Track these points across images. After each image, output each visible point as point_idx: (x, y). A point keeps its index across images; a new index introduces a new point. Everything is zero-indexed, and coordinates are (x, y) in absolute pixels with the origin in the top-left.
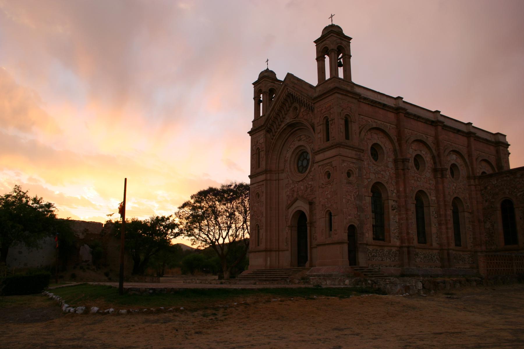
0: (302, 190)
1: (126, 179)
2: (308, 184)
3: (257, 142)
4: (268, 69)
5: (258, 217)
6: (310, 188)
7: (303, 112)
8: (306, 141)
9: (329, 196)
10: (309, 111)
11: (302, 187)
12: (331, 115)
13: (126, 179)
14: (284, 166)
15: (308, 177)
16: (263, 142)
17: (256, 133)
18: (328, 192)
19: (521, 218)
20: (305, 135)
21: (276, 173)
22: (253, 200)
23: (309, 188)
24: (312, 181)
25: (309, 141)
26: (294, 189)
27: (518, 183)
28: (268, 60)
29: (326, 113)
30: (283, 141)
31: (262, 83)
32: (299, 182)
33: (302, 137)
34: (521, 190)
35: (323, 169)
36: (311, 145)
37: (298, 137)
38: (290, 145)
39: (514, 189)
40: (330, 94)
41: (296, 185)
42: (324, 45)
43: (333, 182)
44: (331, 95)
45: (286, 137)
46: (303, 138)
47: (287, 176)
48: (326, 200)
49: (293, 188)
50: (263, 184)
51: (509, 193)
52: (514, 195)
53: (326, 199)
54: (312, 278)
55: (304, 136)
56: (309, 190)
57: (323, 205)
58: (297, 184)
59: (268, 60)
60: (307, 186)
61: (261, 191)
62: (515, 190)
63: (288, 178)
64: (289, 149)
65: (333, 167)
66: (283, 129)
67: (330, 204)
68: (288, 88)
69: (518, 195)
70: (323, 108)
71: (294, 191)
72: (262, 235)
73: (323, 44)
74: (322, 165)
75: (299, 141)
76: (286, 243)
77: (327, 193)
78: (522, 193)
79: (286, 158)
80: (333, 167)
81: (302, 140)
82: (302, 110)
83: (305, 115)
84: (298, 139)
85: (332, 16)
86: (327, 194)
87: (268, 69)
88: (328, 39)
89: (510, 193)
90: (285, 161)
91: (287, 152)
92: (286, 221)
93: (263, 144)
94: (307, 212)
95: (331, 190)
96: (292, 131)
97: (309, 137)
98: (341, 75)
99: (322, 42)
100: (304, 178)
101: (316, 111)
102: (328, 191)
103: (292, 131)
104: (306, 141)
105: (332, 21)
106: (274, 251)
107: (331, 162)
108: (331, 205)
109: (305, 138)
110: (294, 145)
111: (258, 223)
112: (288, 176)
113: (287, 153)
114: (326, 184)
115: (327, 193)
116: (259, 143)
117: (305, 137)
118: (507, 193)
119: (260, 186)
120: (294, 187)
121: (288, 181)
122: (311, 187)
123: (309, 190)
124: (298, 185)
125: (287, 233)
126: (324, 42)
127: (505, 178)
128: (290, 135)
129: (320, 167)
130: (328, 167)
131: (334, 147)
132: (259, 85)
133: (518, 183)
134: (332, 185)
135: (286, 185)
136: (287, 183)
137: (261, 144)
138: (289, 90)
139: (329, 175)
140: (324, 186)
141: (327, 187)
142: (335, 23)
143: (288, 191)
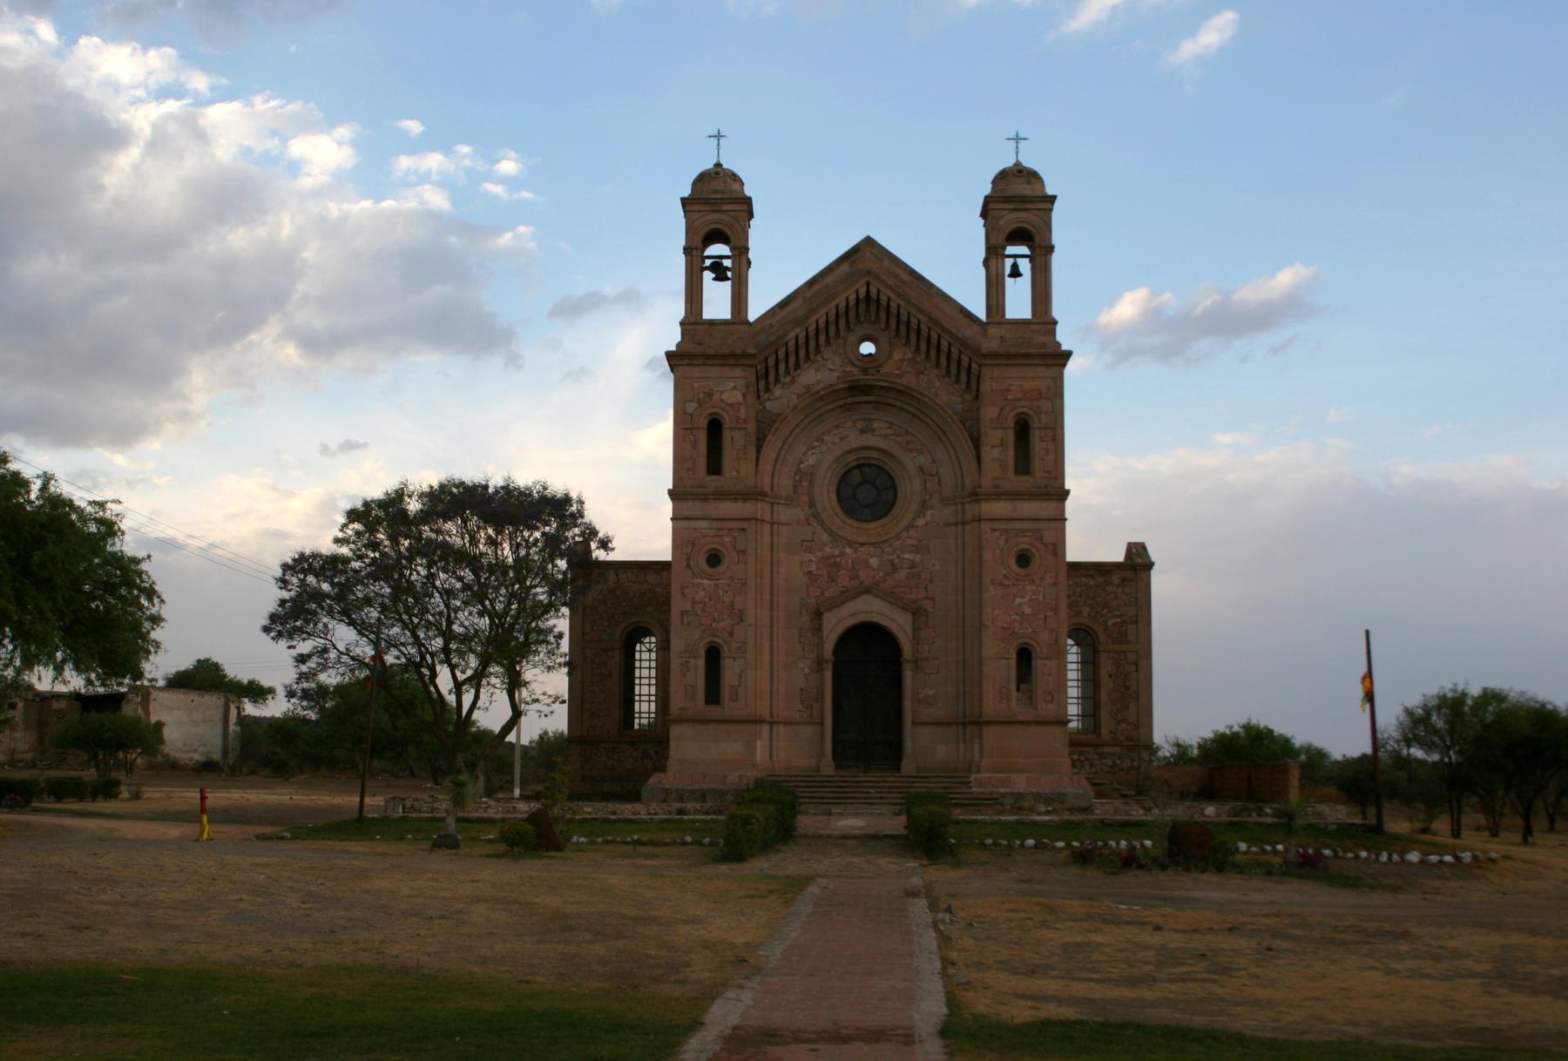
0: (873, 569)
1: (1367, 632)
2: (899, 557)
3: (710, 395)
4: (718, 165)
5: (714, 620)
6: (906, 571)
7: (903, 361)
8: (896, 442)
9: (1027, 610)
10: (925, 368)
11: (874, 562)
12: (1043, 416)
13: (1367, 632)
14: (795, 486)
15: (899, 539)
16: (740, 404)
17: (704, 365)
18: (1025, 600)
19: (1110, 676)
20: (890, 423)
21: (772, 504)
22: (688, 566)
23: (902, 568)
24: (916, 553)
25: (908, 443)
26: (838, 560)
27: (1113, 595)
28: (719, 136)
29: (1024, 403)
30: (806, 418)
31: (731, 214)
32: (862, 544)
33: (875, 424)
34: (1117, 613)
35: (1007, 541)
36: (914, 457)
37: (863, 420)
38: (824, 434)
39: (1103, 610)
40: (1042, 363)
41: (848, 550)
42: (1021, 222)
43: (1041, 579)
44: (1046, 365)
45: (822, 410)
46: (880, 428)
47: (807, 520)
48: (1017, 618)
49: (831, 556)
50: (744, 530)
51: (1089, 615)
52: (1101, 621)
53: (1017, 614)
54: (1101, 803)
55: (887, 425)
56: (903, 573)
57: (1003, 628)
58: (850, 547)
59: (719, 136)
60: (896, 561)
61: (734, 547)
62: (1105, 611)
63: (809, 524)
64: (816, 444)
65: (1045, 545)
66: (830, 390)
67: (1030, 630)
68: (872, 280)
69: (1110, 623)
70: (1012, 388)
71: (836, 565)
72: (740, 676)
73: (1015, 215)
74: (1006, 531)
75: (862, 431)
76: (802, 702)
77: (1018, 601)
78: (1119, 620)
79: (802, 466)
80: (1045, 545)
81: (877, 432)
82: (897, 356)
83: (909, 372)
84: (860, 427)
85: (1017, 139)
86: (1020, 604)
87: (718, 165)
88: (1036, 212)
89: (1093, 615)
90: (796, 474)
91: (809, 449)
92: (800, 642)
93: (743, 409)
94: (904, 631)
95: (1034, 597)
96: (849, 400)
97: (907, 433)
98: (1018, 303)
99: (1016, 210)
100: (885, 537)
101: (987, 386)
102: (1023, 597)
103: (849, 400)
104: (896, 442)
105: (1017, 153)
106: (767, 722)
107: (1038, 530)
108: (1034, 632)
109: (890, 432)
110: (842, 439)
111: (717, 640)
112: (811, 518)
113: (810, 453)
114: (1018, 580)
115: (1018, 601)
116: (722, 400)
117: (890, 428)
118: (1086, 615)
119: (725, 532)
120: (837, 553)
121: (813, 533)
122: (912, 567)
123: (903, 573)
124: (856, 554)
125: (805, 675)
126: (1022, 215)
127: (1083, 579)
128: (833, 409)
129: (997, 534)
130: (1027, 539)
131: (1052, 497)
132: (717, 216)
133: (1113, 595)
134: (1037, 586)
135: (803, 541)
136: (811, 539)
137: (731, 405)
138: (873, 291)
139: (1024, 560)
140: (1010, 583)
141: (1020, 587)
142: (1028, 163)
143: (811, 561)
